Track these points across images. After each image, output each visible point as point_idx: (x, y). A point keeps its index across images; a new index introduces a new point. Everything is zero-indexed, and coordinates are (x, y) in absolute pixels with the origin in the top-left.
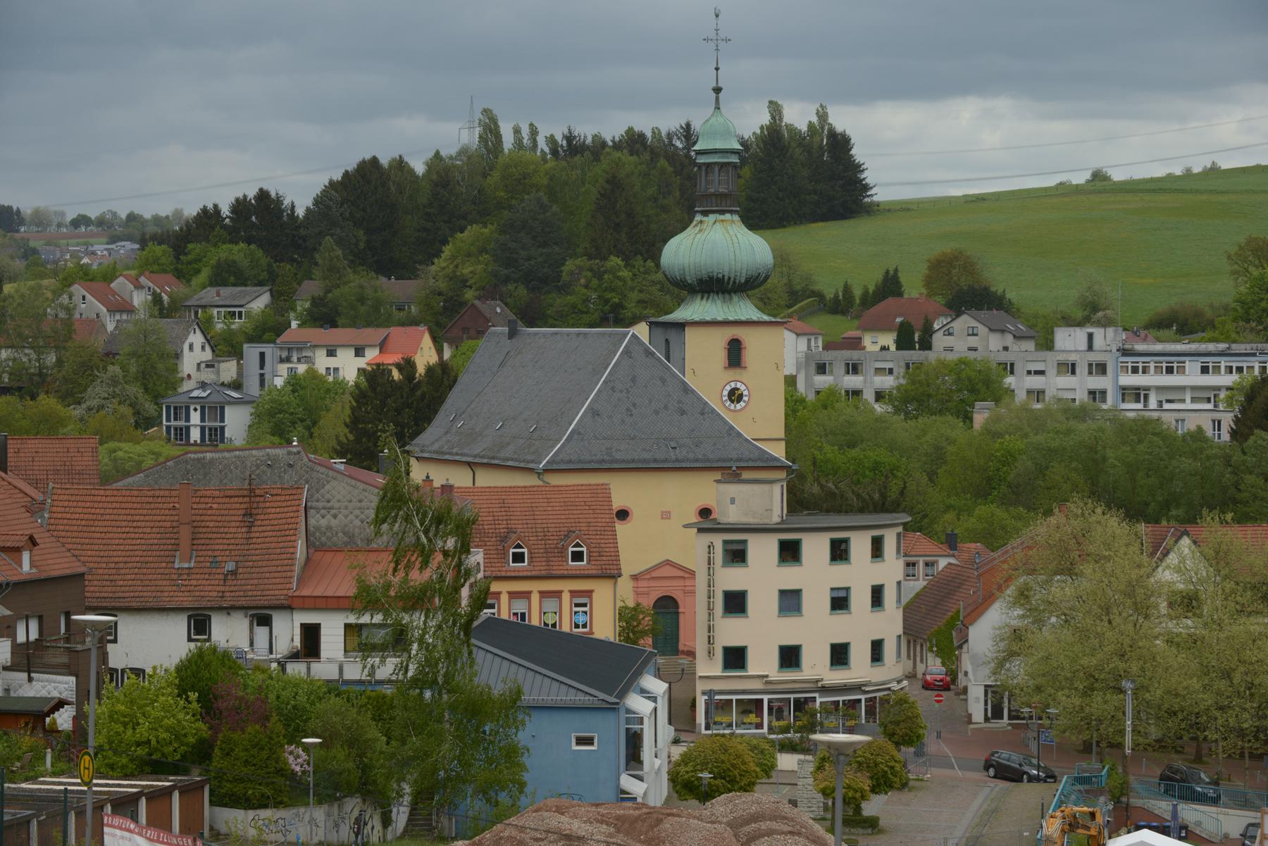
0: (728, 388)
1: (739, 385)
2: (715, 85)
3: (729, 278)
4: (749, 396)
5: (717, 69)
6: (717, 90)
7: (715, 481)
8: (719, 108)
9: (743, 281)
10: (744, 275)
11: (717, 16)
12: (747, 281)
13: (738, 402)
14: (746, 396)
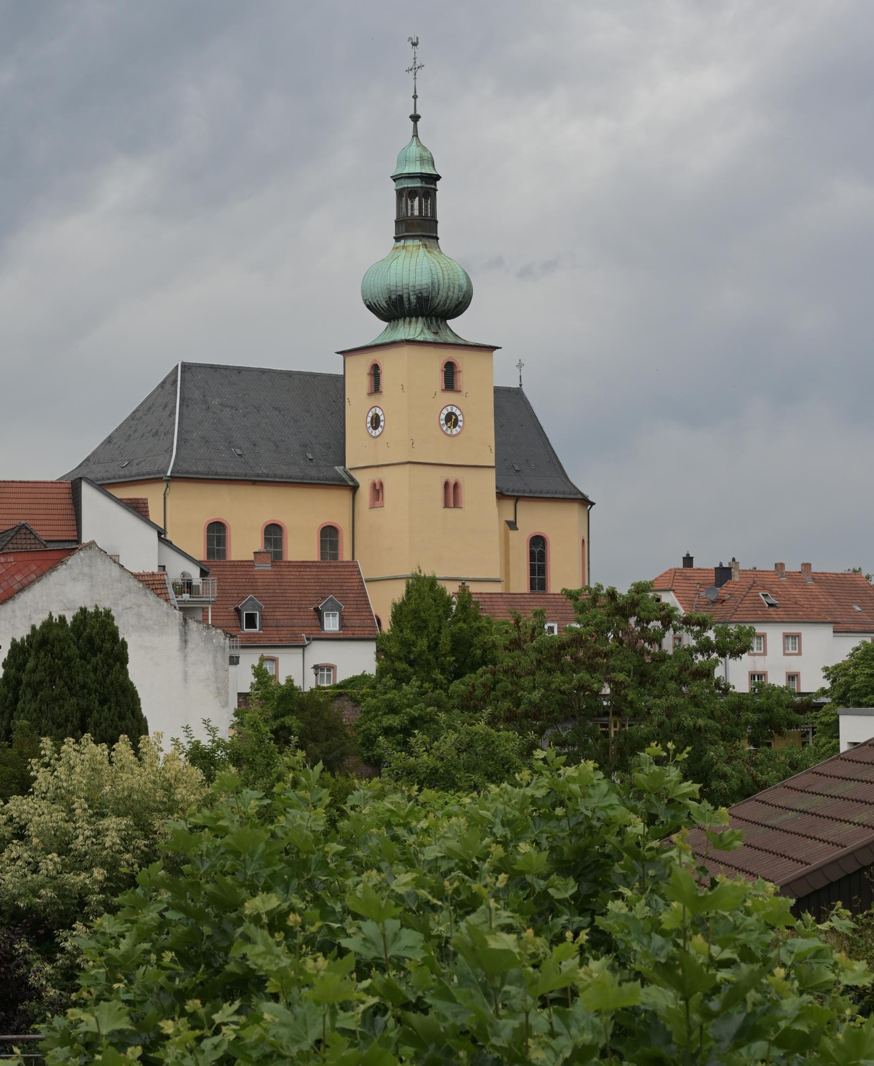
0: (445, 412)
1: (454, 410)
2: (412, 113)
3: (375, 304)
4: (463, 421)
5: (415, 97)
6: (415, 118)
7: (372, 507)
8: (417, 136)
9: (386, 306)
10: (382, 299)
11: (415, 44)
12: (388, 305)
13: (454, 427)
14: (461, 421)
